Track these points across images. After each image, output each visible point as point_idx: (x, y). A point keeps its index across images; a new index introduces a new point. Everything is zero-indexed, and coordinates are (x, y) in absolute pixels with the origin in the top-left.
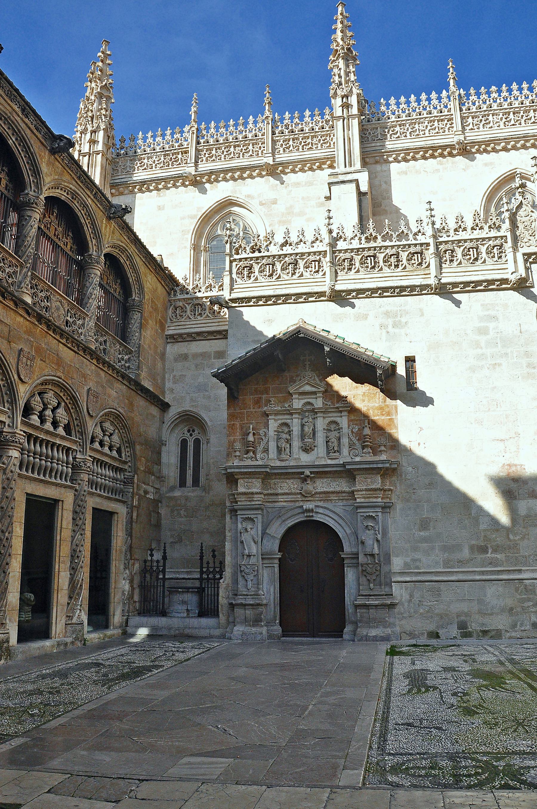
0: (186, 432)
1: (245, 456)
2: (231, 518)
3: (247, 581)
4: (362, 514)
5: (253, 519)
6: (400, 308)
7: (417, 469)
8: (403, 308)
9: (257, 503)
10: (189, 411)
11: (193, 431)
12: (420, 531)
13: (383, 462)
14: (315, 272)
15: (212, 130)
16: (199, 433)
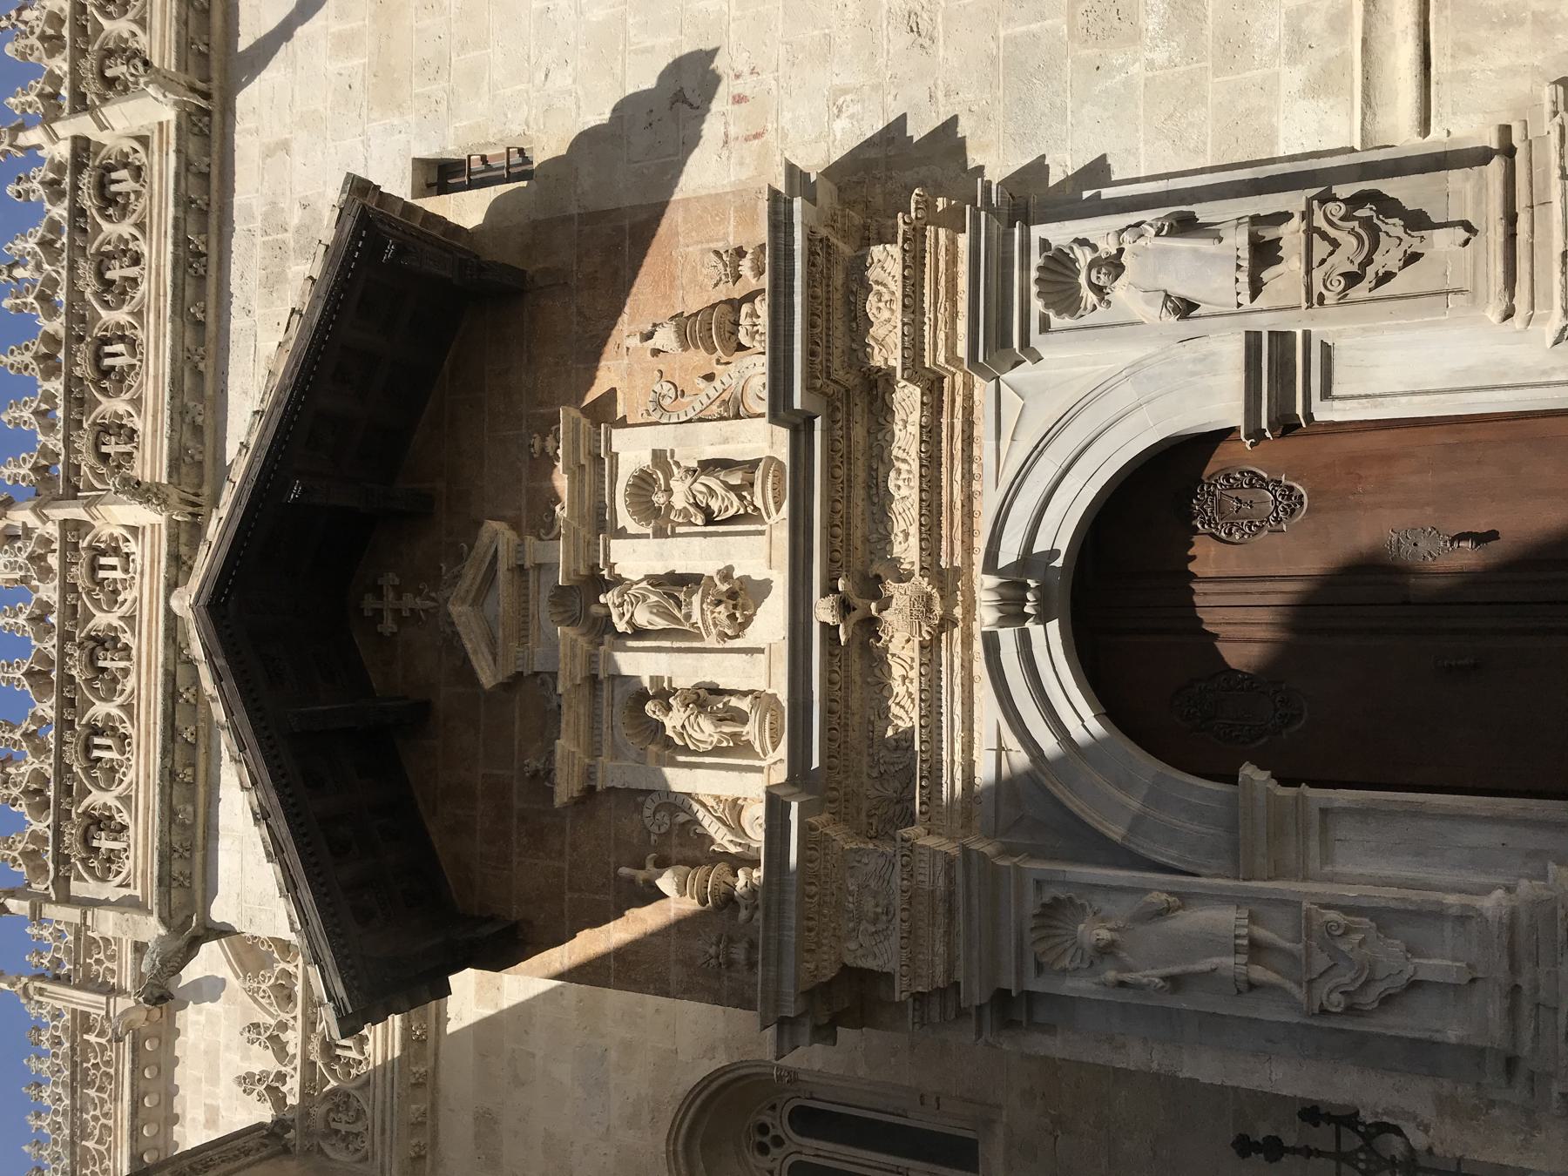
0: (765, 1162)
1: (743, 914)
2: (1049, 1029)
3: (1414, 985)
4: (1035, 324)
5: (1044, 905)
6: (258, 233)
7: (845, 92)
8: (257, 225)
9: (960, 879)
10: (672, 1138)
11: (763, 1129)
12: (1135, 37)
13: (780, 222)
14: (126, 571)
15: (45, 933)
16: (773, 1108)
